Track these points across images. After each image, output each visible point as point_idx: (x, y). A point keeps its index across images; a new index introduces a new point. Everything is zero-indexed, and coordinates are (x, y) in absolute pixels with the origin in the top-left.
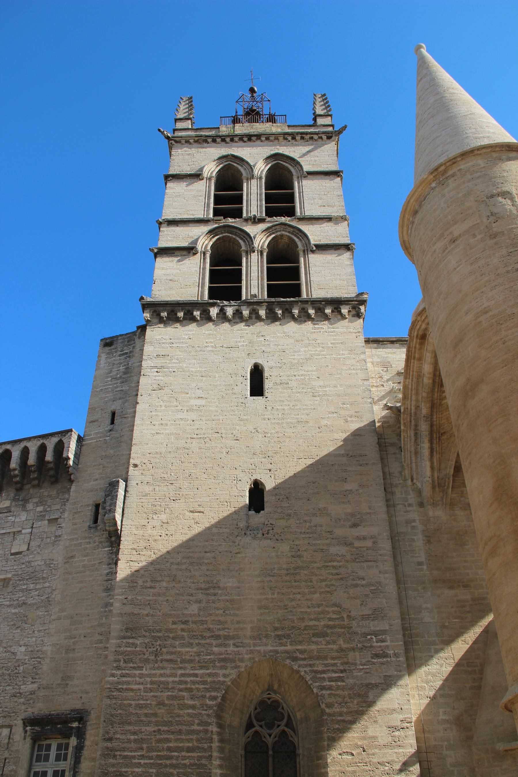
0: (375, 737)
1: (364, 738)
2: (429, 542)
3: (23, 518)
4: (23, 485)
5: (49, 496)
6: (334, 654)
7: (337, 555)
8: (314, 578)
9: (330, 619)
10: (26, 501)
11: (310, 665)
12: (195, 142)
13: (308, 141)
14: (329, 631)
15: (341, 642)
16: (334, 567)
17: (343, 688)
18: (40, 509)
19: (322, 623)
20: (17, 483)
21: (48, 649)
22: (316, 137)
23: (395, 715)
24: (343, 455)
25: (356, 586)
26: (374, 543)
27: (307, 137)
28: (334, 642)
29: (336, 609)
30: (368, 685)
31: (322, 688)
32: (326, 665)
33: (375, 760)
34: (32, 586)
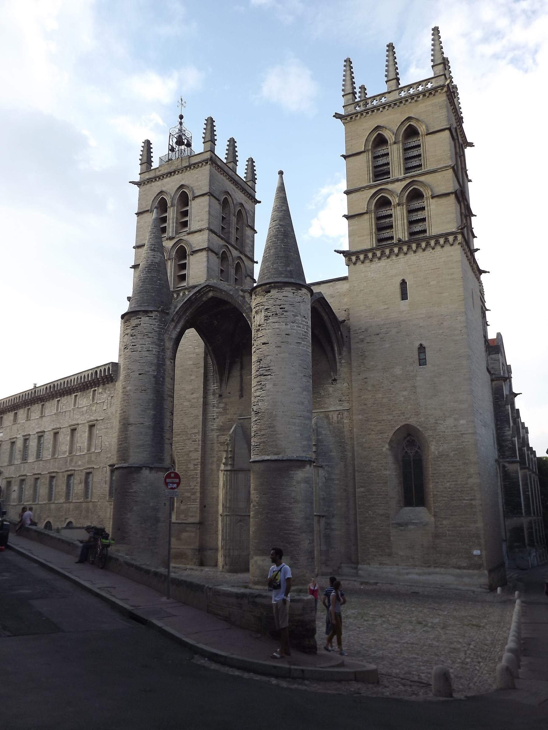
1: (187, 468)
5: (111, 387)
8: (179, 415)
9: (182, 429)
10: (105, 389)
11: (175, 445)
14: (181, 433)
16: (185, 410)
17: (182, 452)
18: (109, 392)
19: (180, 430)
20: (102, 383)
21: (112, 443)
22: (200, 165)
23: (196, 461)
24: (192, 364)
25: (190, 417)
26: (198, 400)
28: (182, 437)
29: (184, 425)
31: (178, 452)
33: (189, 474)
34: (108, 422)
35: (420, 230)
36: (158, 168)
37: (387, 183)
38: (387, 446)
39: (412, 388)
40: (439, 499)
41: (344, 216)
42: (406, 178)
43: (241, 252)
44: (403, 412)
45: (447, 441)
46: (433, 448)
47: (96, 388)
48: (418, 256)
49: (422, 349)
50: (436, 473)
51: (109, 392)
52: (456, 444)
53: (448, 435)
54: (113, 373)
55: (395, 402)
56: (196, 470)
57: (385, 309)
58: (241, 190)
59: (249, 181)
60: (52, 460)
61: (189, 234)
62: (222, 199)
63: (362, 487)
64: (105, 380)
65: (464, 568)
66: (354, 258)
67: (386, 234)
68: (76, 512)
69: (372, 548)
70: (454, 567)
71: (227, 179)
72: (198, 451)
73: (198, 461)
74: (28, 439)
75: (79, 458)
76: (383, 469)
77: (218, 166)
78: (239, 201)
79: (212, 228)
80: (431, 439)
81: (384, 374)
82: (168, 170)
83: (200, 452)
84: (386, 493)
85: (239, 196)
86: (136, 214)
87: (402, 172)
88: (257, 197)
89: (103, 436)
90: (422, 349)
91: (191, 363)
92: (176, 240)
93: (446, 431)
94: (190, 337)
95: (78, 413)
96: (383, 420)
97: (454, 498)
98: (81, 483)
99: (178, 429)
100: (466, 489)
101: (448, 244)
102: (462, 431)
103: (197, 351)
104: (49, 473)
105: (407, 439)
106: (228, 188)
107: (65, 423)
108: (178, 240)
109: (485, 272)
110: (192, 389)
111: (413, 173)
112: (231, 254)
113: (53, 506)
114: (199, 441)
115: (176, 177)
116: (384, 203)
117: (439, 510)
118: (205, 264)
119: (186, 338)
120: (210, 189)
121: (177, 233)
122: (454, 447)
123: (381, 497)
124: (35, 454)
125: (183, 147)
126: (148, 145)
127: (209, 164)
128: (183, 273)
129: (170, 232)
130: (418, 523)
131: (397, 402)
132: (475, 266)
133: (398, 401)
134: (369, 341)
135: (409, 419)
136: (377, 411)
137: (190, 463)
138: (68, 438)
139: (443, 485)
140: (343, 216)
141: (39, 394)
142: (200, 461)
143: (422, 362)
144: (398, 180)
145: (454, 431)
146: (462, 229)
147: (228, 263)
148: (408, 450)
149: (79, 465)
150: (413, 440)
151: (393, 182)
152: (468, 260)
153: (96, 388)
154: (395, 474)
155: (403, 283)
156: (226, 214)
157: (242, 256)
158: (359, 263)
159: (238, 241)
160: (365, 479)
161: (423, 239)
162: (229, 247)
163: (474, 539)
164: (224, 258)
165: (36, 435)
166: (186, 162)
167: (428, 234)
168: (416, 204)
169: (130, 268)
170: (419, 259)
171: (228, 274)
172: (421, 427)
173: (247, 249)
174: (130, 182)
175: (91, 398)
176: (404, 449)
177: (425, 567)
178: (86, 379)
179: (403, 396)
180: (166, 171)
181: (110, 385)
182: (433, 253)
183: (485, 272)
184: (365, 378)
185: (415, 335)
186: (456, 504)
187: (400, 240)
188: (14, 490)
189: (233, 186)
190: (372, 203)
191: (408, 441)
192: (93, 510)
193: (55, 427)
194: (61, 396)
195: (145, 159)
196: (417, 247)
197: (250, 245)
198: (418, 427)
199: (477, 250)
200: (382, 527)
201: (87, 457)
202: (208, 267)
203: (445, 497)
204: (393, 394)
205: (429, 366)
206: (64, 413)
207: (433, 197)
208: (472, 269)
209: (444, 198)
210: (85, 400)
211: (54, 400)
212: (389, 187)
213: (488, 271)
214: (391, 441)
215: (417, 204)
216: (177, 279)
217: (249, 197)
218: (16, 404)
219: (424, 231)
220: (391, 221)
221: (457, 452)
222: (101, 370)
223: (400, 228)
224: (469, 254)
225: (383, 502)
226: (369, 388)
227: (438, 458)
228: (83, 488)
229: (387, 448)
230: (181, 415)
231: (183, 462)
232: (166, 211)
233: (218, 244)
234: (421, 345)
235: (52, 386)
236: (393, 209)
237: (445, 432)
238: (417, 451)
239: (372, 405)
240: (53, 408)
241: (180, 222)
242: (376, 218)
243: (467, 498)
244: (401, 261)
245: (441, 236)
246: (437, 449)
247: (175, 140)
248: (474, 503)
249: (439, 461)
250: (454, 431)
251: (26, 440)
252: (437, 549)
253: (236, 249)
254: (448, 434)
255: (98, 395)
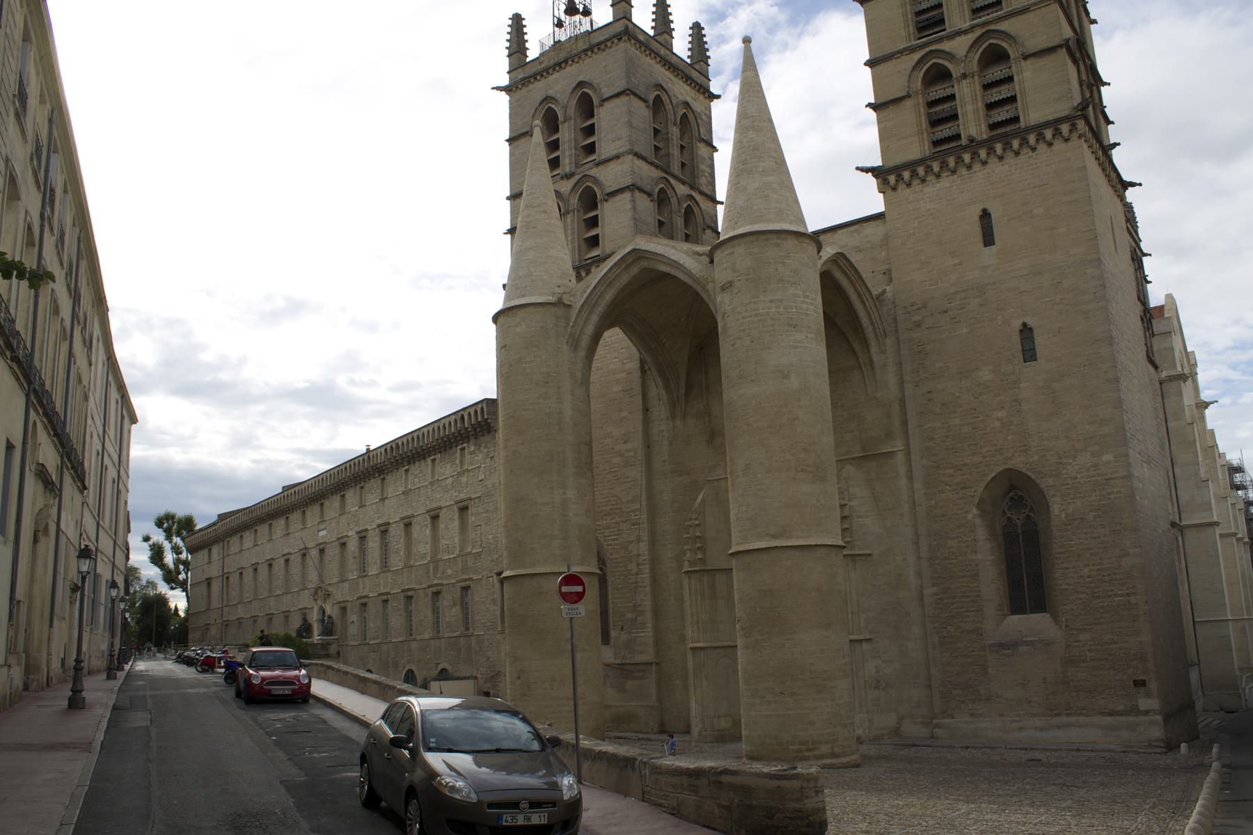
0: (631, 570)
2: (671, 445)
3: (481, 457)
4: (477, 435)
6: (614, 525)
7: (616, 464)
9: (612, 505)
10: (480, 445)
11: (603, 533)
12: (523, 85)
13: (604, 51)
15: (617, 518)
16: (615, 472)
18: (486, 451)
19: (609, 508)
20: (473, 435)
21: (499, 535)
22: (609, 44)
24: (621, 391)
25: (625, 482)
26: (636, 452)
27: (603, 47)
28: (614, 518)
29: (615, 498)
30: (629, 541)
31: (608, 545)
32: (610, 532)
33: (631, 581)
35: (1008, 117)
36: (537, 58)
37: (941, 40)
38: (975, 511)
39: (1014, 403)
40: (1071, 598)
41: (869, 105)
42: (973, 27)
43: (692, 188)
44: (999, 447)
45: (1080, 493)
46: (1055, 508)
47: (464, 445)
48: (1006, 167)
49: (1026, 331)
50: (1064, 553)
51: (486, 451)
52: (1098, 498)
53: (1082, 482)
54: (490, 417)
55: (983, 432)
56: (641, 574)
57: (955, 265)
58: (684, 80)
59: (697, 62)
60: (404, 570)
61: (598, 164)
62: (651, 98)
63: (934, 585)
64: (478, 430)
65: (1121, 714)
66: (892, 179)
67: (945, 131)
68: (451, 653)
69: (955, 689)
70: (1103, 714)
71: (657, 63)
72: (643, 541)
73: (643, 558)
74: (365, 537)
75: (448, 564)
76: (969, 552)
77: (640, 42)
78: (681, 98)
79: (637, 149)
80: (1053, 493)
81: (963, 382)
82: (554, 59)
83: (646, 543)
84: (978, 594)
85: (681, 91)
86: (507, 141)
87: (967, 17)
88: (714, 89)
89: (483, 526)
90: (1026, 331)
91: (620, 389)
92: (577, 177)
93: (1079, 476)
94: (613, 343)
95: (439, 489)
96: (965, 465)
97: (1098, 594)
98: (454, 605)
99: (606, 506)
100: (1118, 577)
101: (1061, 139)
102: (1106, 474)
103: (628, 366)
104: (403, 591)
105: (1009, 496)
106: (660, 78)
107: (420, 507)
108: (581, 178)
109: (1133, 185)
110: (625, 435)
111: (987, 17)
112: (675, 192)
113: (414, 645)
114: (643, 523)
115: (570, 70)
116: (939, 75)
117: (1072, 617)
118: (630, 214)
119: (609, 345)
120: (628, 82)
121: (578, 165)
122: (1093, 504)
123: (967, 600)
124: (378, 561)
125: (577, 18)
126: (517, 23)
127: (625, 41)
128: (593, 233)
129: (566, 165)
130: (1034, 641)
131: (988, 430)
132: (1113, 175)
133: (989, 428)
134: (931, 326)
135: (1011, 459)
136: (952, 449)
137: (632, 562)
138: (428, 532)
139: (1077, 572)
140: (866, 106)
141: (375, 462)
142: (647, 557)
143: (1029, 354)
144: (960, 33)
145: (1094, 476)
146: (1083, 109)
147: (671, 208)
148: (1012, 514)
149: (449, 576)
150: (1021, 497)
151: (952, 36)
152: (1099, 164)
153: (465, 445)
154: (991, 558)
155: (985, 215)
156: (660, 123)
157: (694, 194)
158: (901, 186)
159: (686, 167)
160: (939, 571)
161: (1015, 134)
162: (671, 180)
163: (1136, 662)
164: (662, 200)
165: (377, 530)
166: (585, 43)
167: (1022, 124)
168: (997, 72)
169: (504, 233)
170: (1010, 171)
171: (672, 227)
172: (1033, 473)
173: (703, 180)
174: (493, 88)
175: (458, 462)
176: (1006, 514)
177: (1051, 716)
178: (447, 430)
179: (998, 419)
180: (552, 62)
181: (487, 438)
182: (1034, 157)
183: (1133, 185)
184: (929, 392)
185: (1013, 308)
186: (1101, 604)
187: (972, 140)
188: (353, 622)
189: (668, 74)
190: (918, 77)
191: (1012, 499)
192: (478, 649)
193: (405, 514)
194: (409, 463)
195: (515, 46)
196: (1004, 149)
197: (707, 174)
198: (1029, 473)
199: (1116, 145)
200: (972, 651)
201: (460, 562)
202: (635, 219)
203: (1082, 593)
204: (979, 417)
205: (1041, 363)
206: (417, 491)
207: (1026, 57)
208: (1109, 181)
209: (1047, 56)
210: (448, 466)
211: (400, 471)
212: (946, 46)
213: (1138, 182)
214: (981, 500)
215: (999, 72)
216: (584, 246)
217: (699, 89)
218: (343, 481)
219: (1016, 119)
220: (954, 107)
221: (1100, 513)
222: (469, 414)
223: (971, 117)
224: (1100, 153)
225: (972, 609)
226: (937, 410)
227: (1066, 525)
228: (459, 613)
229: (974, 515)
230: (609, 481)
231: (619, 560)
232: (556, 130)
233: (650, 177)
234: (1025, 325)
235: (394, 446)
236: (955, 85)
237: (1076, 478)
238: (1028, 516)
239: (944, 439)
240: (398, 483)
241: (582, 147)
242: (927, 104)
243: (1120, 593)
244: (977, 176)
245: (1047, 124)
246: (1064, 510)
247: (563, 8)
248: (1133, 599)
249: (1069, 530)
250: (1094, 476)
251: (362, 538)
252: (1071, 683)
253: (684, 183)
254: (1082, 481)
255: (469, 457)
